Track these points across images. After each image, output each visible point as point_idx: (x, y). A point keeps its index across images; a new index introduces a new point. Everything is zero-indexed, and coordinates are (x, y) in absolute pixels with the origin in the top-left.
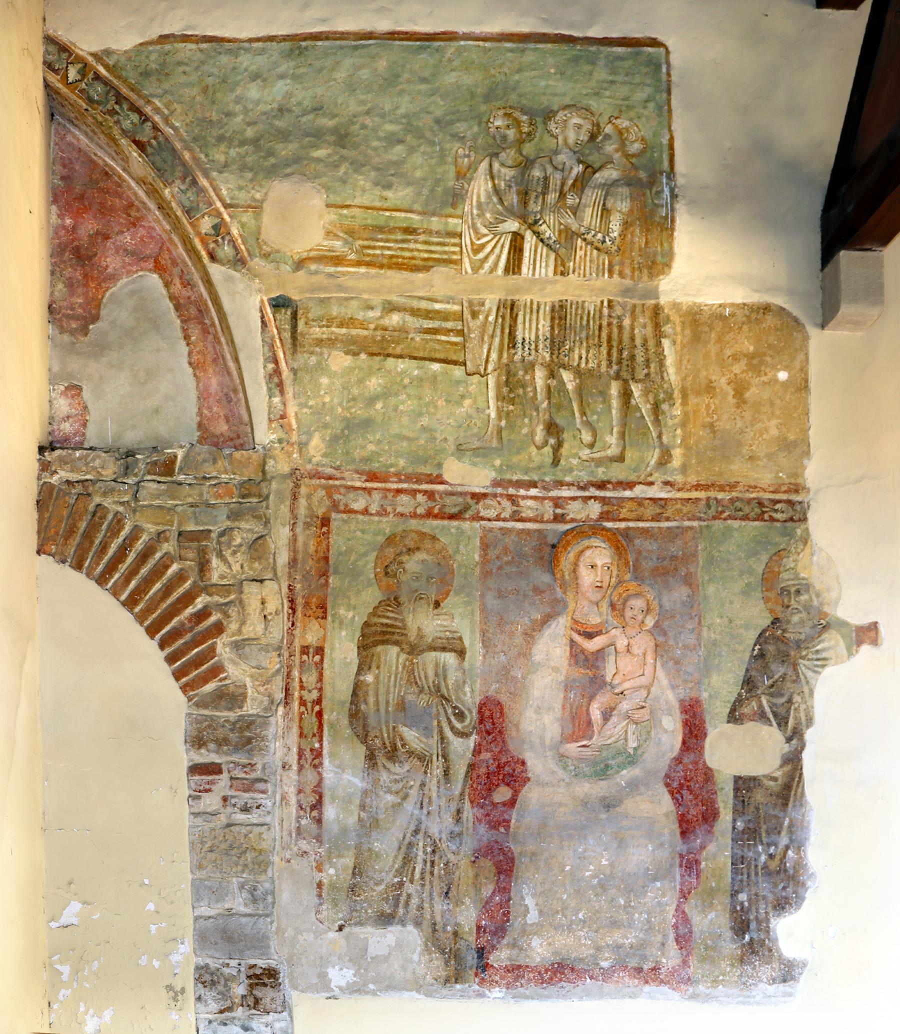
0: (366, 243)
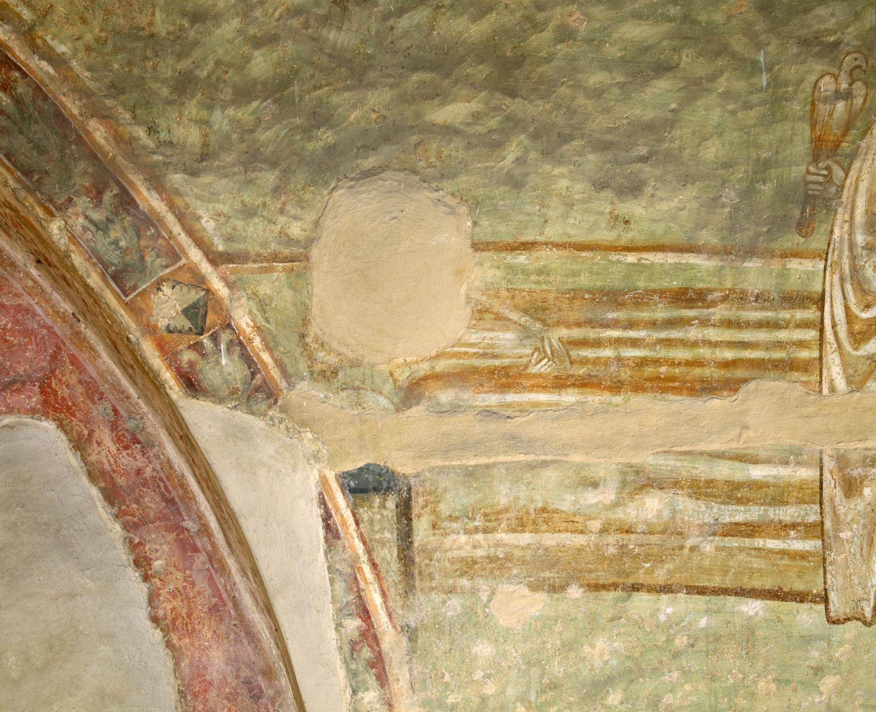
0: (576, 333)
